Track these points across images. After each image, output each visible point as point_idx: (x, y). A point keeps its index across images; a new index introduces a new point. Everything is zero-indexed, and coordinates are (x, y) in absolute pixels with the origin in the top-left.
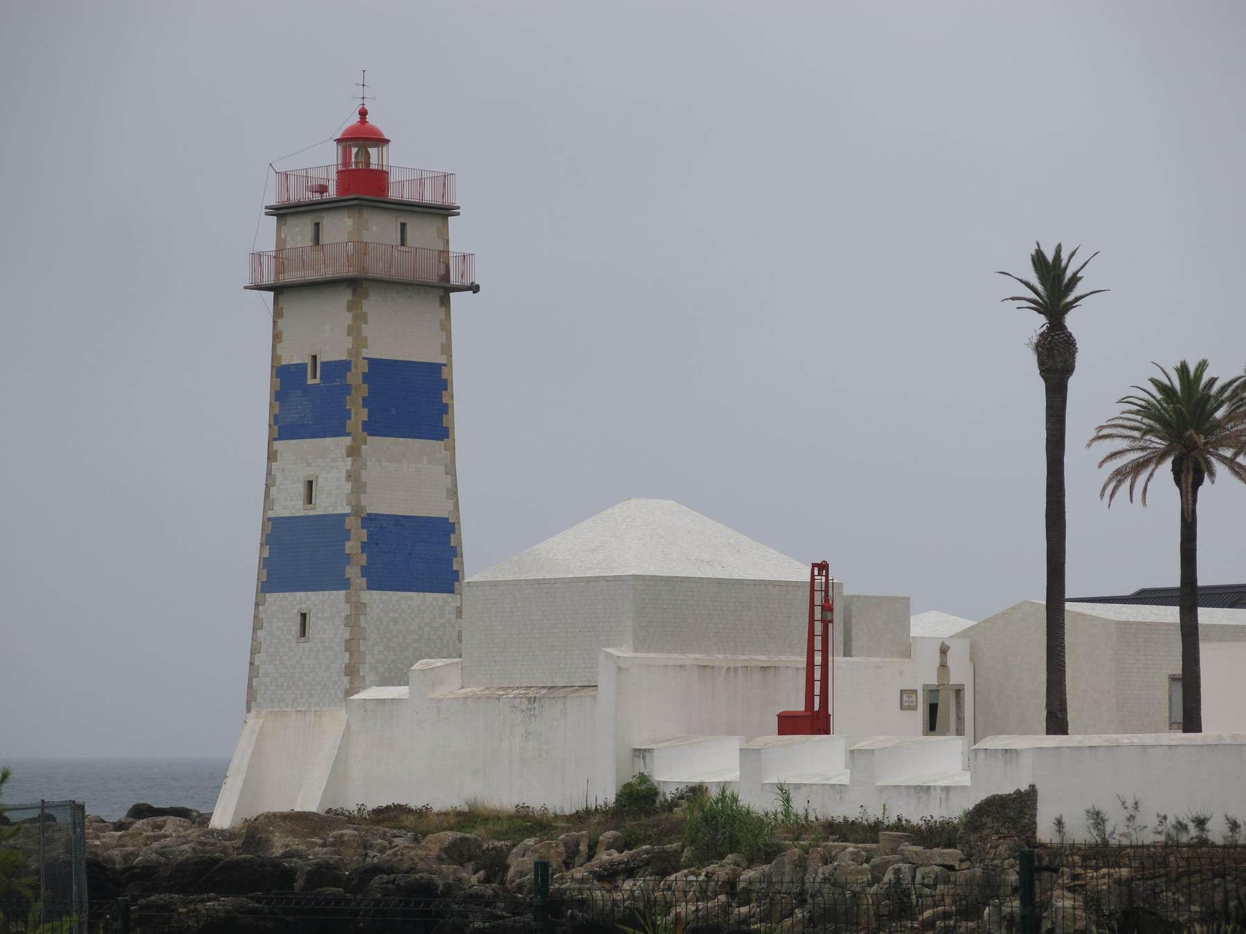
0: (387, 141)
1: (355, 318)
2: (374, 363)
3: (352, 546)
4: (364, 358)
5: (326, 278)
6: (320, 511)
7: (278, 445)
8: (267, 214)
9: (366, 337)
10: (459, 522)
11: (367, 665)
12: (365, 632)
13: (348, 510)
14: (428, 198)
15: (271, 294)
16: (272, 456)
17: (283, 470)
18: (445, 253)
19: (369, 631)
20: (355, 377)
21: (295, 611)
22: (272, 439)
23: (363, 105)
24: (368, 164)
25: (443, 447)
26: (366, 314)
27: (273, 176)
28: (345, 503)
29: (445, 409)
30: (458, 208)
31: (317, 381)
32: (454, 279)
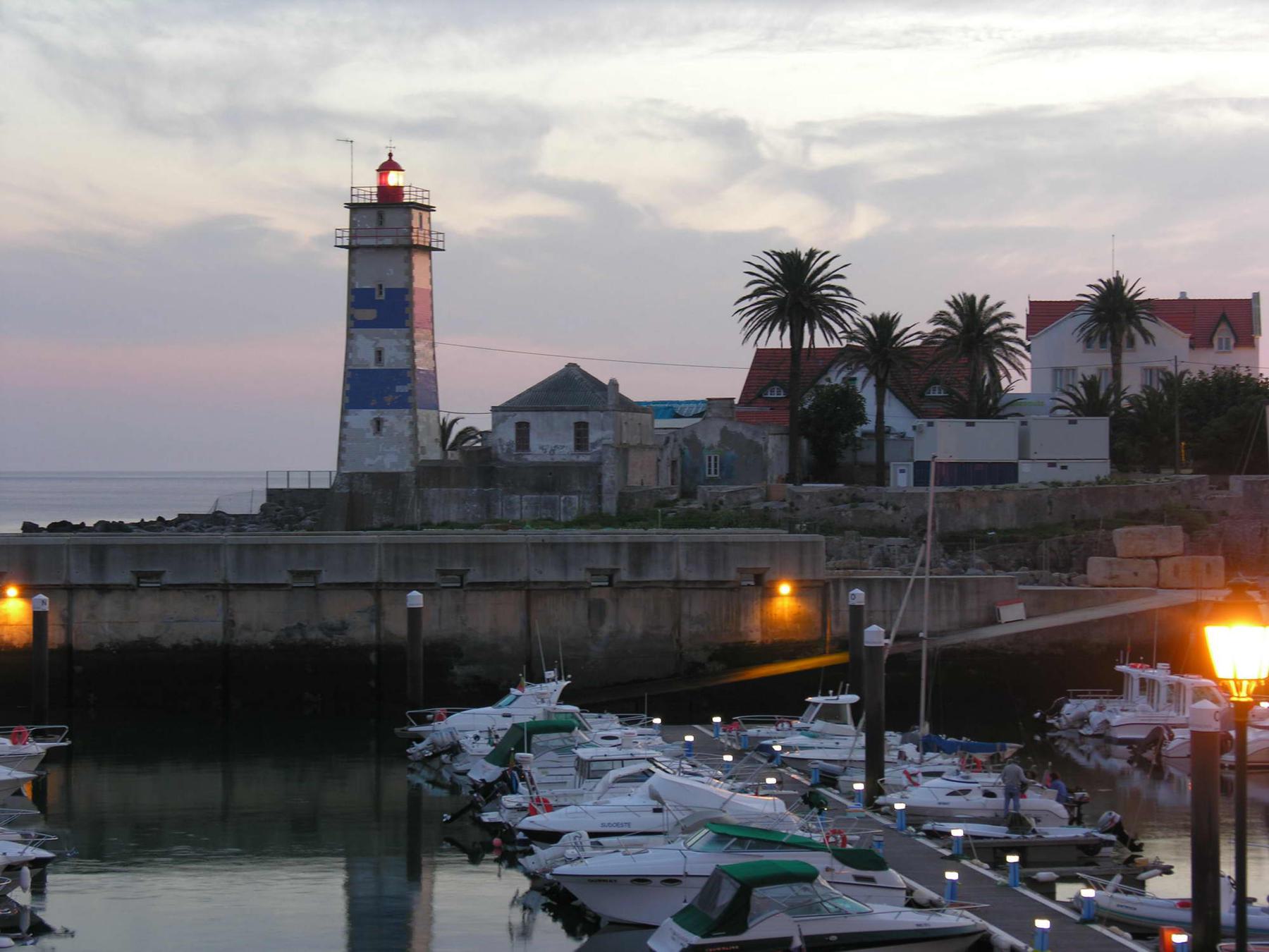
6: (386, 367)
7: (353, 331)
13: (408, 366)
15: (347, 251)
16: (350, 336)
22: (349, 328)
31: (383, 297)
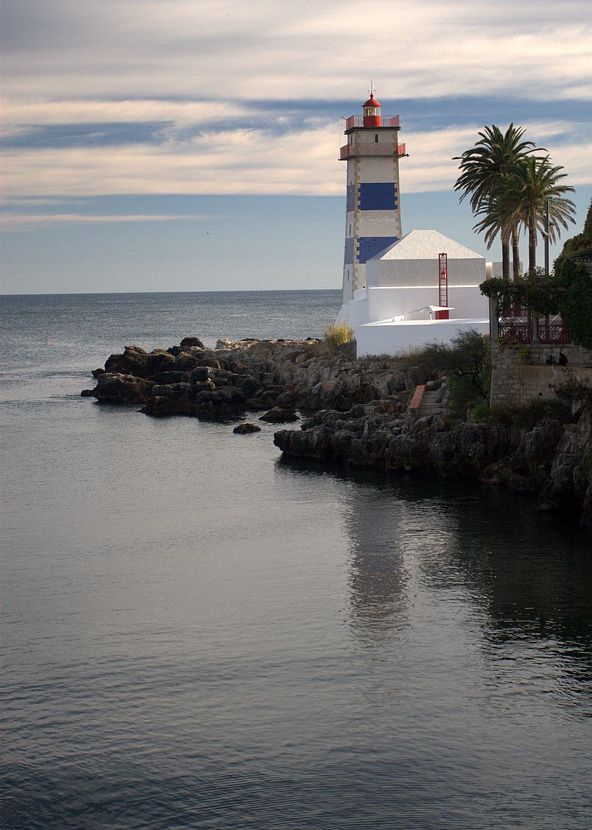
29: (396, 199)
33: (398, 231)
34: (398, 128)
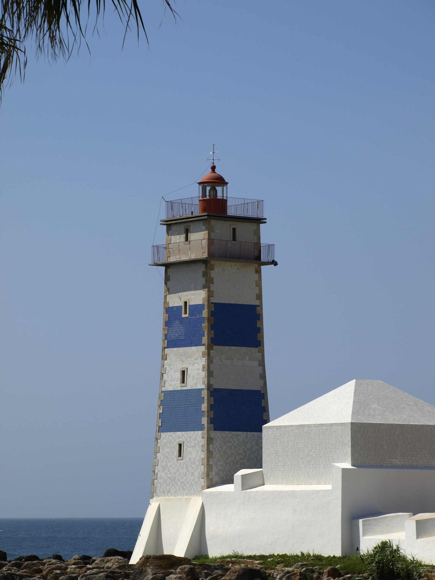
0: (227, 183)
1: (207, 281)
2: (216, 305)
3: (204, 407)
4: (212, 303)
5: (191, 259)
6: (189, 387)
7: (167, 351)
8: (161, 224)
9: (213, 291)
10: (267, 393)
11: (214, 472)
12: (212, 454)
13: (203, 387)
14: (251, 214)
15: (164, 267)
17: (170, 365)
18: (258, 245)
19: (215, 453)
20: (205, 313)
21: (176, 443)
23: (213, 163)
24: (216, 195)
25: (257, 351)
26: (212, 279)
27: (164, 203)
28: (201, 383)
29: (259, 330)
30: (266, 219)
32: (263, 258)
33: (262, 382)
34: (259, 221)
